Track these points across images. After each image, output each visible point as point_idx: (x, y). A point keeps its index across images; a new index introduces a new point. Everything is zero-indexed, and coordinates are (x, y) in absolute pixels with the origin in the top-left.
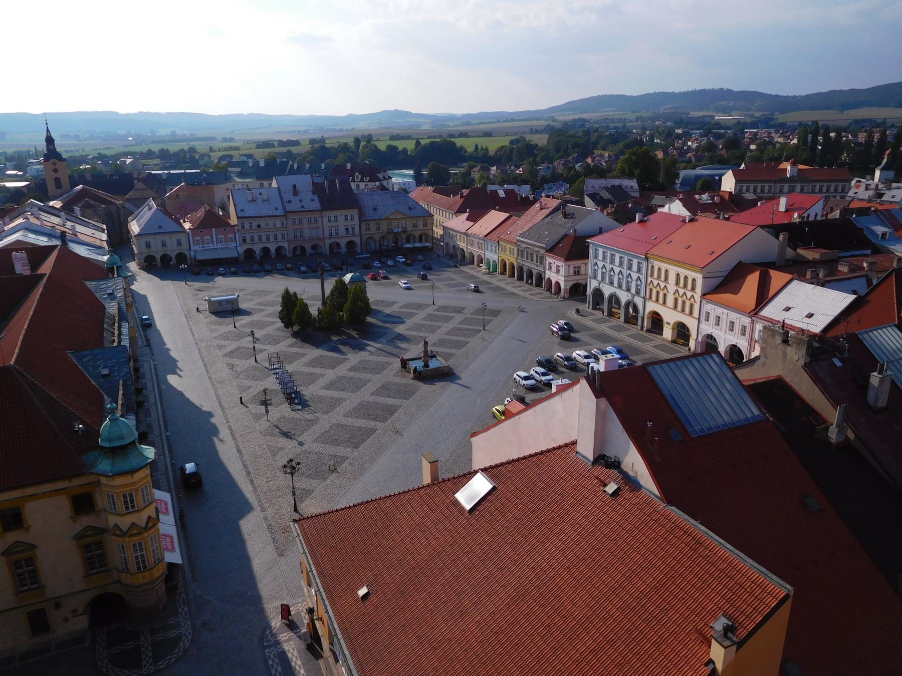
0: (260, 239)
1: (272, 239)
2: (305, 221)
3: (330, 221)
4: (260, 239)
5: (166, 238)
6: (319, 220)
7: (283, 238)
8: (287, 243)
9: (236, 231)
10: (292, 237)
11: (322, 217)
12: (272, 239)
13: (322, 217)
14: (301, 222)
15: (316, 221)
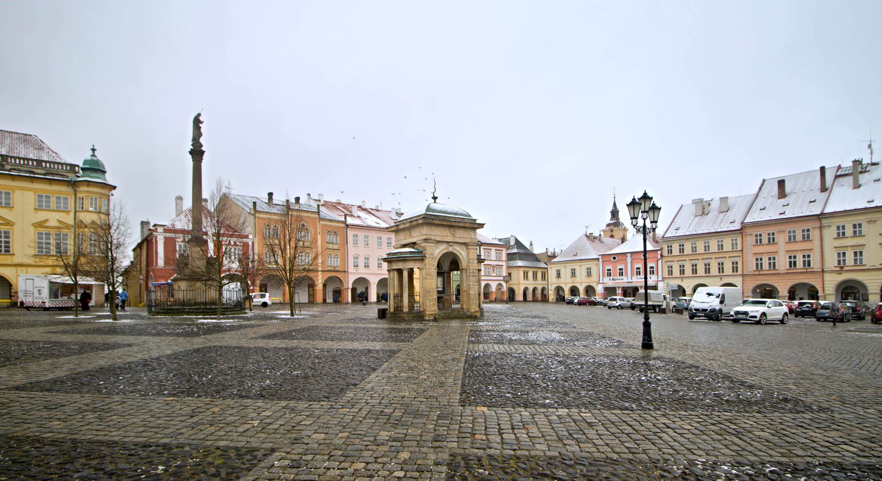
0: (694, 271)
1: (688, 271)
2: (781, 239)
3: (841, 235)
4: (694, 271)
5: (576, 266)
6: (815, 235)
7: (735, 269)
8: (740, 279)
9: (659, 257)
10: (751, 267)
11: (821, 228)
12: (688, 271)
13: (821, 228)
14: (772, 241)
15: (806, 238)
